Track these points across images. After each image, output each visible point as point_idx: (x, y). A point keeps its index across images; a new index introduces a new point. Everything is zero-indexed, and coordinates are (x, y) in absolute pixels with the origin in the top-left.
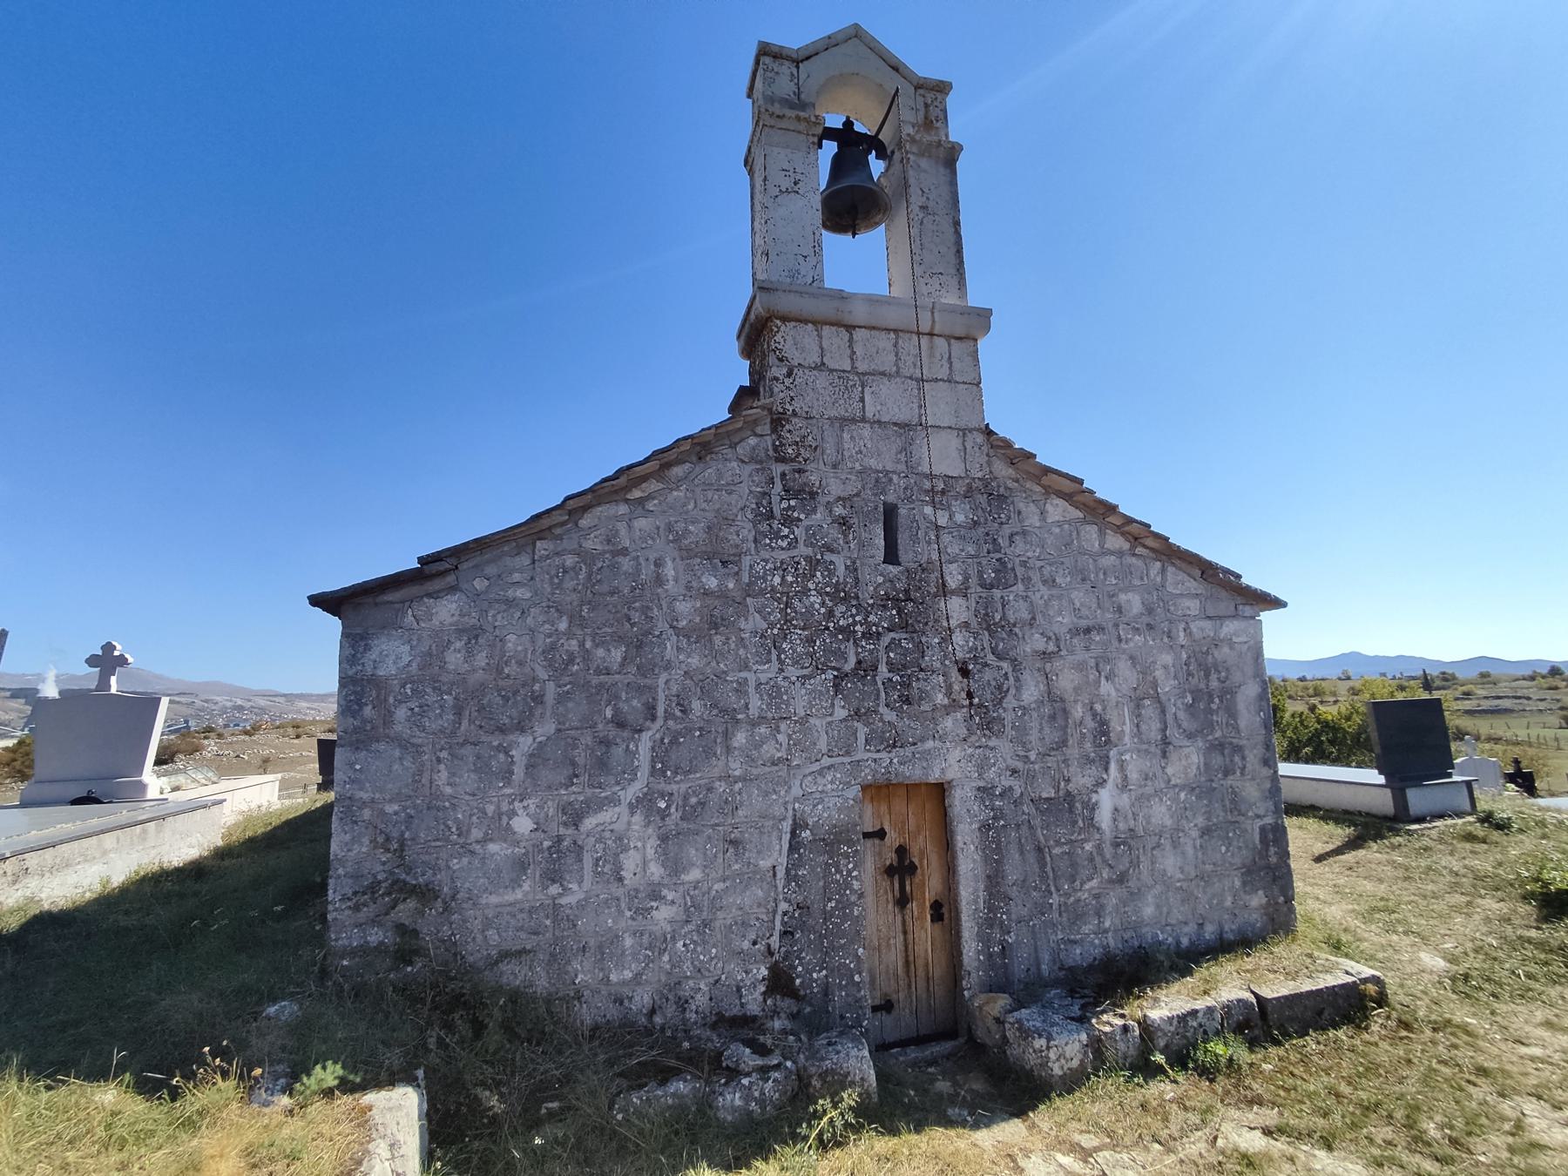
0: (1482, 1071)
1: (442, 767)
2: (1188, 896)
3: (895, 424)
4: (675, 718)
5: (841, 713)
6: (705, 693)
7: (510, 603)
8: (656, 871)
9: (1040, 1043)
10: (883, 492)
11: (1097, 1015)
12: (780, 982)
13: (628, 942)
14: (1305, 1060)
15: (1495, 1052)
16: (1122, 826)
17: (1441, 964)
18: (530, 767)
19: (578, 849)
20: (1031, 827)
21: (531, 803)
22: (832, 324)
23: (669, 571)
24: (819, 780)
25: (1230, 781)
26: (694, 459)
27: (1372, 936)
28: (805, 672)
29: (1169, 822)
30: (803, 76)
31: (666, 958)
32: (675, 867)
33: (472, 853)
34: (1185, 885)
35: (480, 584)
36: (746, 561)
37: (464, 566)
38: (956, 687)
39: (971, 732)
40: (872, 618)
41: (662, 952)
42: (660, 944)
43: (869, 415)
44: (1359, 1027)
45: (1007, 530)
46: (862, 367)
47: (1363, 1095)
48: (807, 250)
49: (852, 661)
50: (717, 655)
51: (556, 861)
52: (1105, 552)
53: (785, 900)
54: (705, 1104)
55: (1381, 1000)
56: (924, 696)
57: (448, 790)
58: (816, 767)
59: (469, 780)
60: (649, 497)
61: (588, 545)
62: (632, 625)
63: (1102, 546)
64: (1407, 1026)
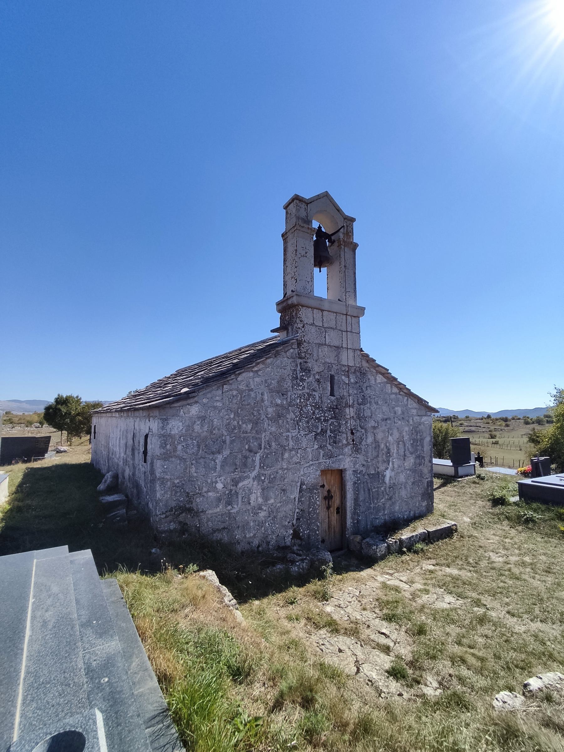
0: (481, 547)
1: (193, 466)
2: (407, 504)
5: (316, 447)
6: (276, 440)
7: (215, 408)
8: (260, 500)
9: (374, 547)
10: (330, 371)
11: (387, 539)
12: (296, 535)
13: (252, 524)
14: (439, 548)
15: (483, 542)
16: (392, 482)
17: (469, 520)
18: (222, 467)
19: (237, 493)
20: (367, 483)
21: (222, 478)
22: (317, 309)
23: (266, 397)
25: (420, 467)
26: (274, 356)
27: (451, 513)
28: (306, 433)
29: (404, 481)
30: (309, 210)
31: (263, 529)
32: (266, 499)
33: (203, 496)
35: (205, 401)
36: (289, 394)
37: (201, 394)
38: (349, 438)
39: (352, 453)
40: (326, 415)
41: (262, 527)
42: (261, 524)
43: (327, 343)
44: (451, 538)
45: (365, 385)
46: (326, 325)
47: (455, 554)
48: (309, 280)
49: (320, 429)
50: (280, 427)
51: (230, 498)
52: (392, 393)
53: (298, 508)
54: (288, 571)
55: (456, 531)
56: (340, 441)
57: (195, 474)
58: (308, 465)
59: (202, 470)
61: (241, 387)
62: (254, 416)
63: (391, 391)
64: (462, 537)
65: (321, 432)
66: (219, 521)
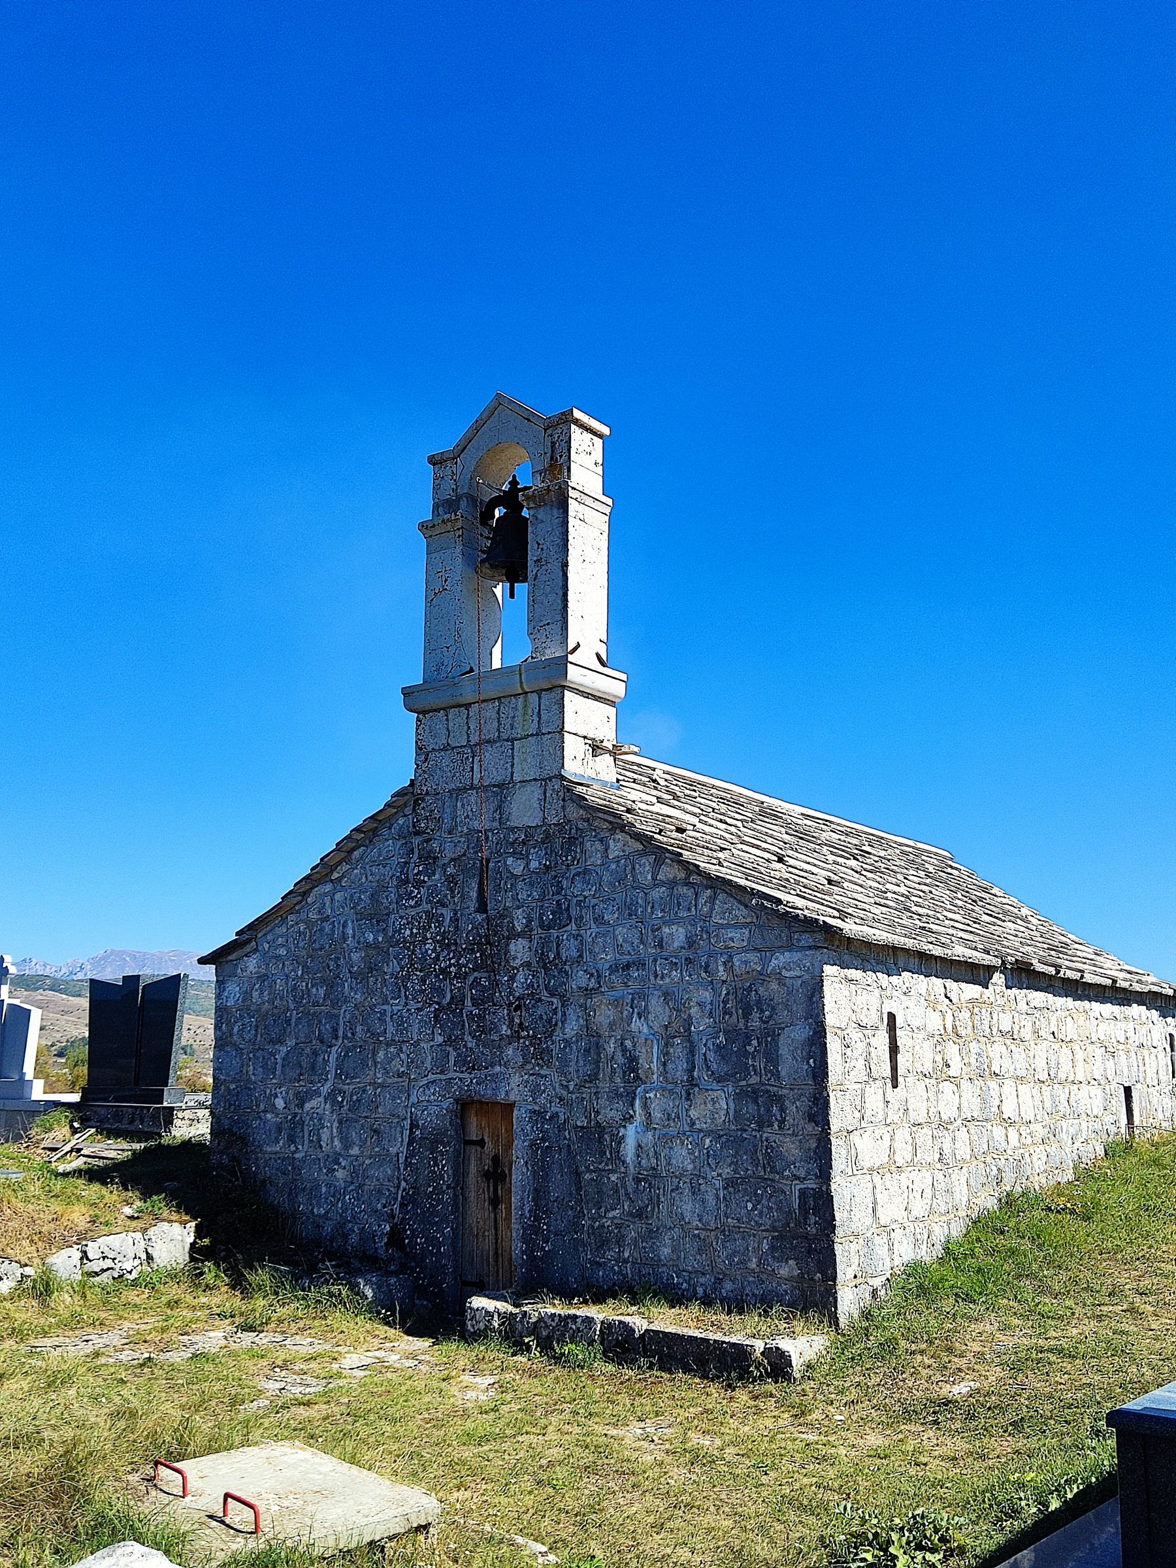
2: (703, 1247)
3: (494, 786)
4: (348, 1038)
5: (439, 1039)
7: (278, 957)
12: (395, 1238)
13: (324, 1189)
24: (427, 1092)
32: (347, 1145)
34: (703, 1234)
42: (337, 1194)
43: (475, 782)
50: (371, 993)
51: (293, 1128)
52: (656, 884)
56: (495, 1028)
60: (343, 876)
65: (449, 1004)
66: (277, 1169)
